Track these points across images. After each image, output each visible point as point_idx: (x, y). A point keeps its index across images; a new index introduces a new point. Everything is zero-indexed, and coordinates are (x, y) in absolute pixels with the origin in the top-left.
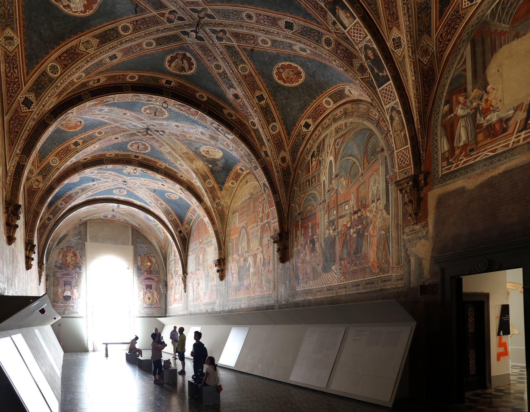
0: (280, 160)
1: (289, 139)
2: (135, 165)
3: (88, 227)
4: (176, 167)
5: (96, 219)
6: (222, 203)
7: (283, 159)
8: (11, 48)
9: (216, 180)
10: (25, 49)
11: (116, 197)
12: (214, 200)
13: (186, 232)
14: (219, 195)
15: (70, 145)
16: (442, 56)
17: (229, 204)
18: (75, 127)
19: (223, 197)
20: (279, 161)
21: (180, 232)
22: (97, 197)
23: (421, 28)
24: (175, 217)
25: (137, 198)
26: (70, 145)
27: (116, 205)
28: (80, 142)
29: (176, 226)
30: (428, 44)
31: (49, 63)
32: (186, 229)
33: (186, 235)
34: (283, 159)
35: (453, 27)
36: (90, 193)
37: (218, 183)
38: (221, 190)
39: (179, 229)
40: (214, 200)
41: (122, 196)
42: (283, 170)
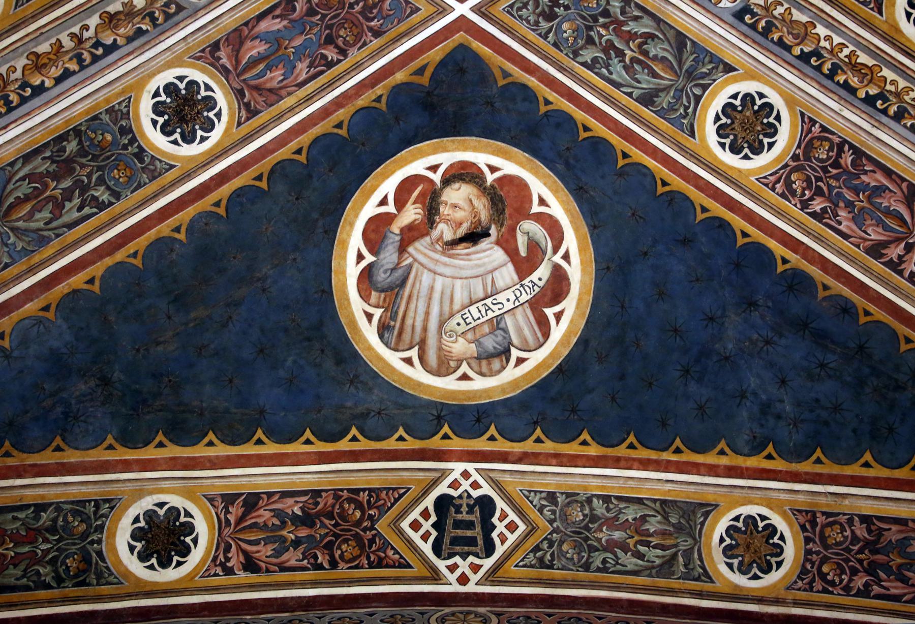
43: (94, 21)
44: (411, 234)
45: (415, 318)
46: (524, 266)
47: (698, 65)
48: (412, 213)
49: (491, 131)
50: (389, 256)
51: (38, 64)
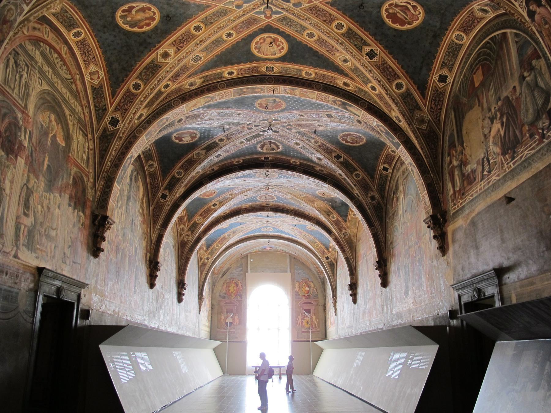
0: (369, 198)
1: (373, 182)
2: (267, 211)
3: (249, 259)
4: (301, 208)
5: (256, 252)
6: (349, 232)
7: (373, 198)
8: (152, 170)
9: (339, 213)
10: (161, 167)
11: (265, 233)
12: (341, 231)
13: (333, 257)
14: (344, 226)
15: (210, 207)
16: (439, 120)
17: (355, 232)
18: (211, 195)
19: (349, 227)
20: (369, 200)
21: (327, 258)
22: (249, 235)
23: (411, 108)
24: (320, 245)
25: (284, 232)
26: (210, 207)
27: (267, 240)
28: (217, 203)
29: (324, 253)
30: (423, 116)
31: (175, 171)
32: (333, 255)
33: (333, 260)
34: (373, 198)
35: (439, 100)
36: (241, 234)
37: (341, 216)
38: (346, 221)
39: (326, 256)
40: (341, 231)
41: (271, 232)
42: (374, 206)
43: (216, 29)
44: (261, 43)
45: (263, 50)
46: (278, 46)
47: (304, 28)
48: (262, 41)
49: (273, 33)
50: (259, 45)
51: (209, 35)
